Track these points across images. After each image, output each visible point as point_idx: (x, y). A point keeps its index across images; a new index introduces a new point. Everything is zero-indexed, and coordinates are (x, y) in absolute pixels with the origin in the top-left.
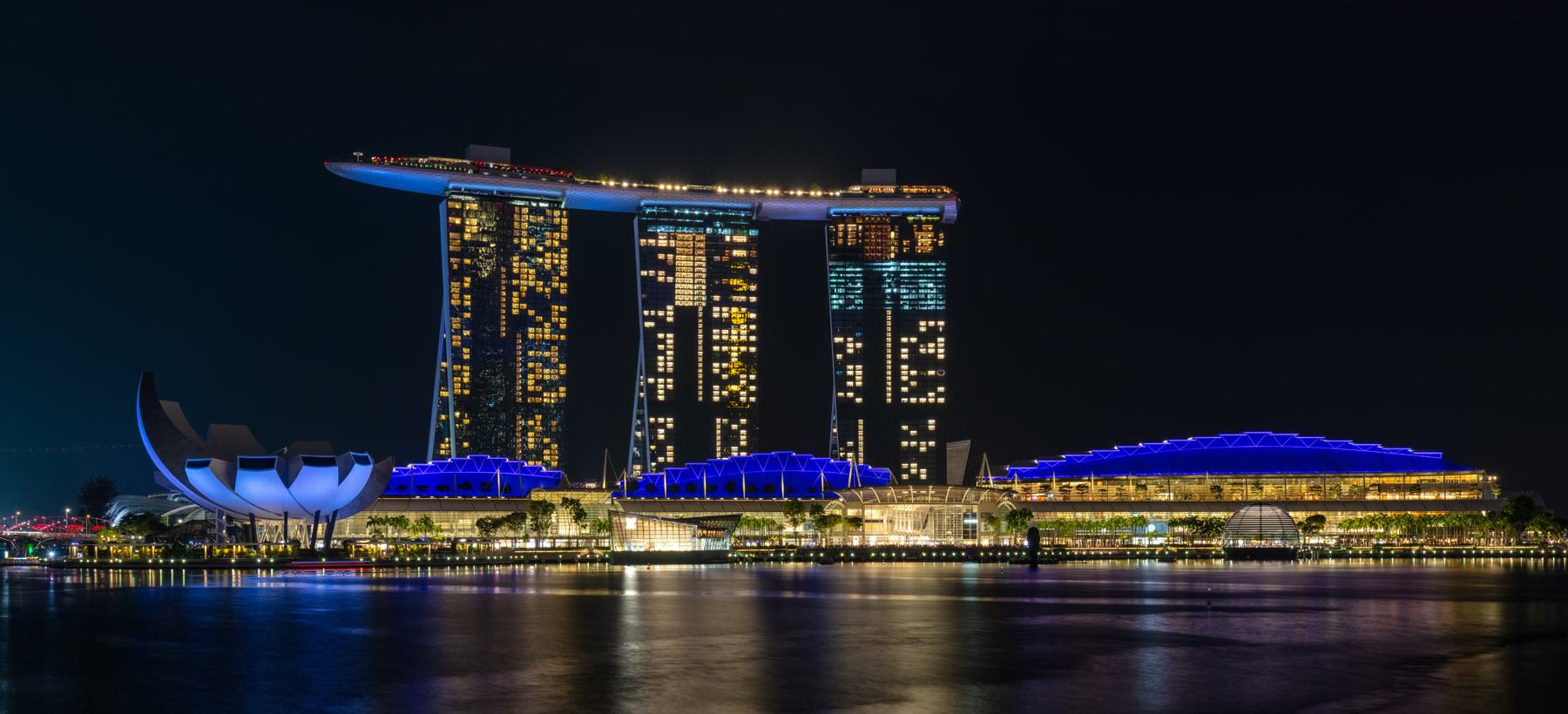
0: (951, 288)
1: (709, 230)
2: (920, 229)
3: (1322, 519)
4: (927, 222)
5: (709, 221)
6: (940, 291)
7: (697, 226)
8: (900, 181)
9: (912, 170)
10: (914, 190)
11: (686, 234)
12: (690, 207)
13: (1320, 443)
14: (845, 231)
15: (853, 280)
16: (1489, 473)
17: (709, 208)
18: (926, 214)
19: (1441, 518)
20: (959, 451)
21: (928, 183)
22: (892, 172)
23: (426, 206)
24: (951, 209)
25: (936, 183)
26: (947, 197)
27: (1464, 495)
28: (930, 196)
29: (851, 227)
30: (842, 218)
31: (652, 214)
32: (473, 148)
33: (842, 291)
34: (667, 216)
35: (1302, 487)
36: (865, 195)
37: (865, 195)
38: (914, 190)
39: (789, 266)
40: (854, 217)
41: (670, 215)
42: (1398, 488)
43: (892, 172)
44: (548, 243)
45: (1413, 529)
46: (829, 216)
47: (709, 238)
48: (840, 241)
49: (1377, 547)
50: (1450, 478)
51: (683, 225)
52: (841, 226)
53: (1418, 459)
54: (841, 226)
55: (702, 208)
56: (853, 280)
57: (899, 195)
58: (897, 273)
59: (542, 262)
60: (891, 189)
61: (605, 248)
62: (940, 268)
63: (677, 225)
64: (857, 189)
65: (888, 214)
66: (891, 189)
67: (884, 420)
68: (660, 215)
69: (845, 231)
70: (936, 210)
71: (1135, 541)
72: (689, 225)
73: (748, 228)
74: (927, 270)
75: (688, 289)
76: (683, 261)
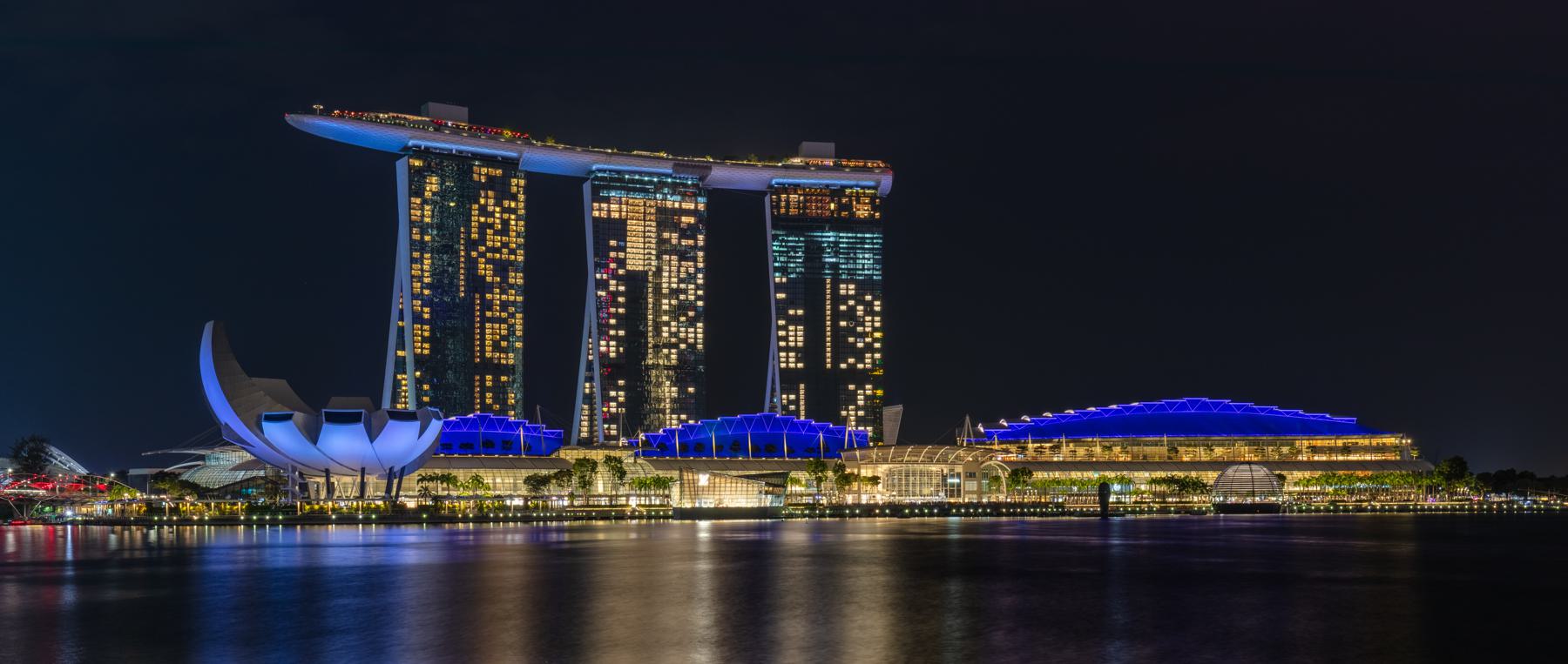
0: (886, 257)
4: (865, 195)
5: (659, 186)
6: (876, 261)
7: (646, 191)
10: (852, 164)
11: (638, 199)
12: (640, 173)
14: (788, 201)
15: (794, 249)
17: (659, 175)
18: (863, 188)
20: (893, 415)
21: (866, 157)
22: (831, 146)
23: (376, 168)
24: (887, 181)
25: (873, 158)
26: (884, 171)
27: (1391, 457)
28: (865, 169)
30: (785, 189)
31: (603, 179)
32: (433, 106)
33: (783, 256)
34: (618, 182)
36: (806, 167)
37: (806, 167)
38: (852, 164)
40: (795, 188)
41: (621, 180)
43: (831, 146)
46: (771, 187)
48: (783, 211)
50: (1374, 442)
51: (635, 190)
52: (784, 196)
53: (1335, 423)
54: (784, 196)
57: (838, 168)
58: (836, 243)
60: (830, 162)
61: (557, 211)
62: (873, 238)
63: (629, 190)
65: (827, 186)
66: (830, 162)
68: (612, 179)
69: (788, 201)
70: (872, 183)
73: (695, 195)
75: (637, 254)
76: (633, 226)
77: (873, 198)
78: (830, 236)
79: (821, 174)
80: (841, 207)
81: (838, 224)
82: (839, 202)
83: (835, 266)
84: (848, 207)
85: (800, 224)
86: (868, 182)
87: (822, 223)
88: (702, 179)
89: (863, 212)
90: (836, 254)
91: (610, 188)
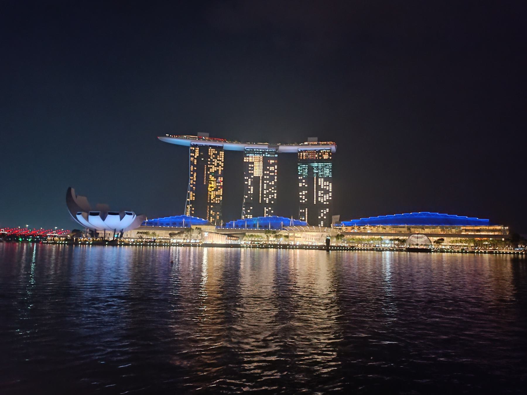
1: (264, 155)
2: (324, 154)
3: (443, 240)
5: (264, 152)
8: (318, 141)
9: (322, 138)
11: (258, 156)
13: (446, 216)
14: (303, 155)
16: (505, 226)
19: (486, 241)
22: (316, 138)
24: (334, 148)
25: (329, 141)
27: (496, 233)
28: (327, 144)
29: (304, 154)
30: (302, 151)
34: (253, 152)
35: (438, 230)
39: (288, 164)
40: (305, 151)
41: (253, 151)
42: (472, 230)
43: (316, 138)
44: (218, 159)
45: (477, 244)
47: (263, 157)
49: (463, 249)
51: (257, 154)
52: (301, 154)
54: (301, 154)
55: (262, 149)
56: (305, 169)
57: (318, 144)
58: (318, 167)
59: (217, 164)
63: (254, 154)
64: (306, 143)
65: (315, 150)
67: (314, 209)
68: (250, 151)
69: (303, 155)
70: (329, 148)
71: (383, 245)
72: (258, 154)
74: (326, 165)
77: (329, 153)
78: (316, 164)
79: (313, 146)
80: (319, 156)
81: (318, 161)
82: (319, 155)
83: (317, 173)
84: (321, 156)
85: (307, 161)
86: (328, 148)
87: (313, 161)
88: (276, 150)
89: (326, 157)
90: (318, 170)
91: (249, 153)
